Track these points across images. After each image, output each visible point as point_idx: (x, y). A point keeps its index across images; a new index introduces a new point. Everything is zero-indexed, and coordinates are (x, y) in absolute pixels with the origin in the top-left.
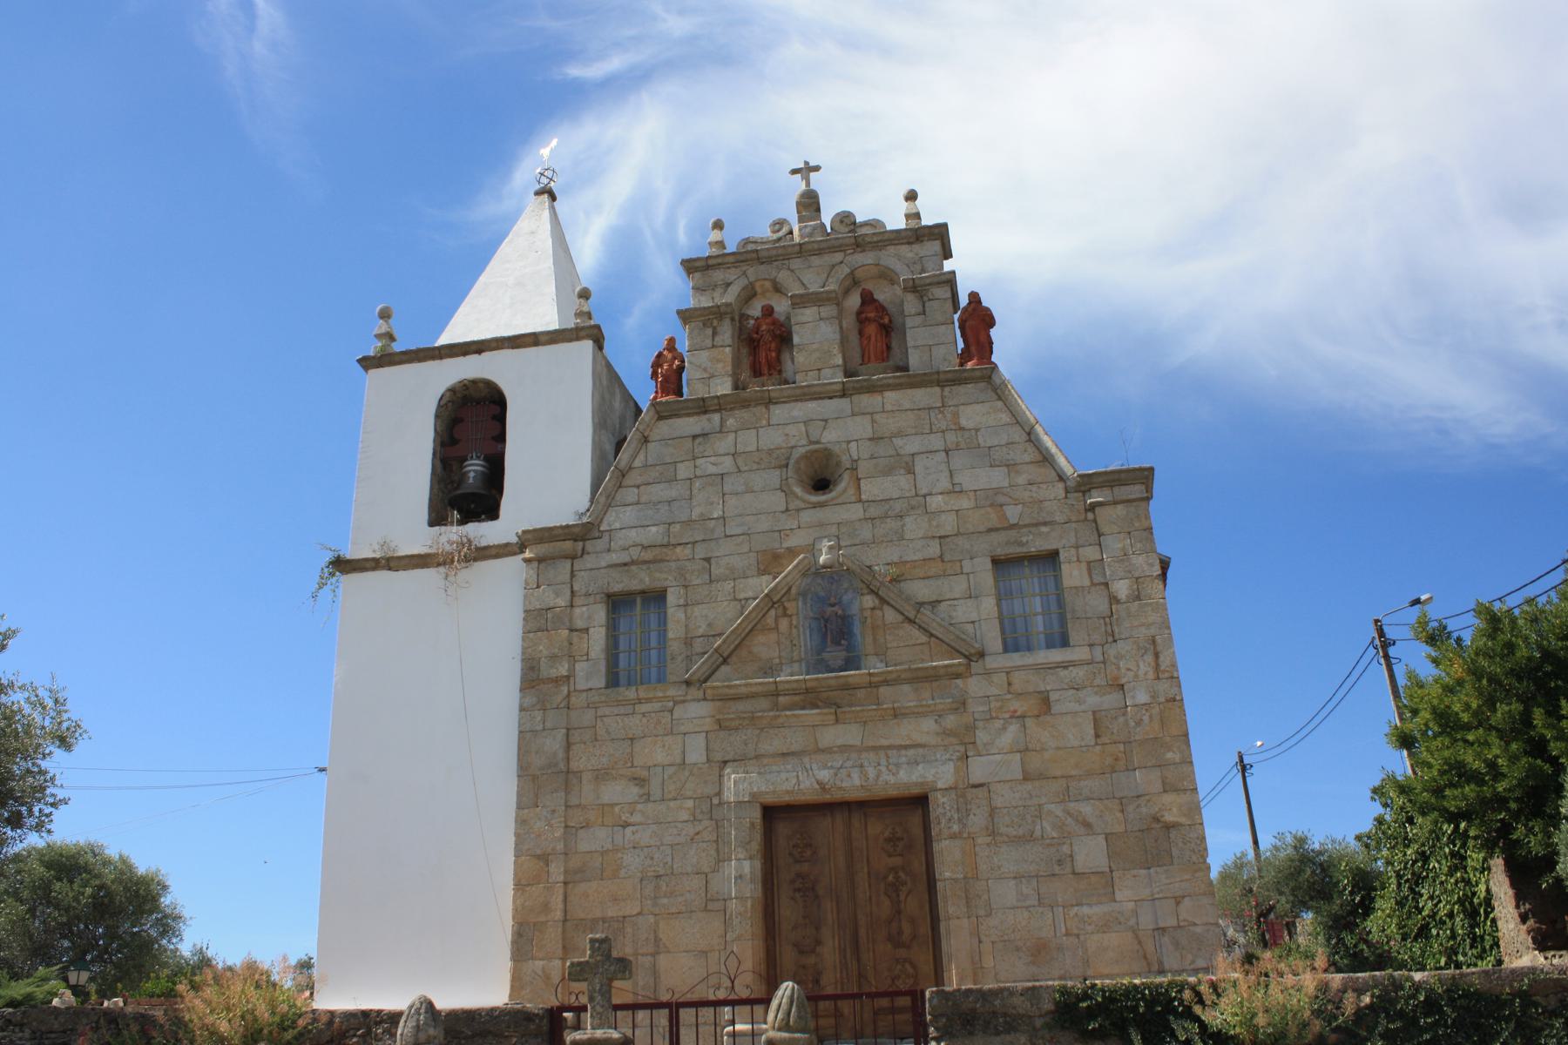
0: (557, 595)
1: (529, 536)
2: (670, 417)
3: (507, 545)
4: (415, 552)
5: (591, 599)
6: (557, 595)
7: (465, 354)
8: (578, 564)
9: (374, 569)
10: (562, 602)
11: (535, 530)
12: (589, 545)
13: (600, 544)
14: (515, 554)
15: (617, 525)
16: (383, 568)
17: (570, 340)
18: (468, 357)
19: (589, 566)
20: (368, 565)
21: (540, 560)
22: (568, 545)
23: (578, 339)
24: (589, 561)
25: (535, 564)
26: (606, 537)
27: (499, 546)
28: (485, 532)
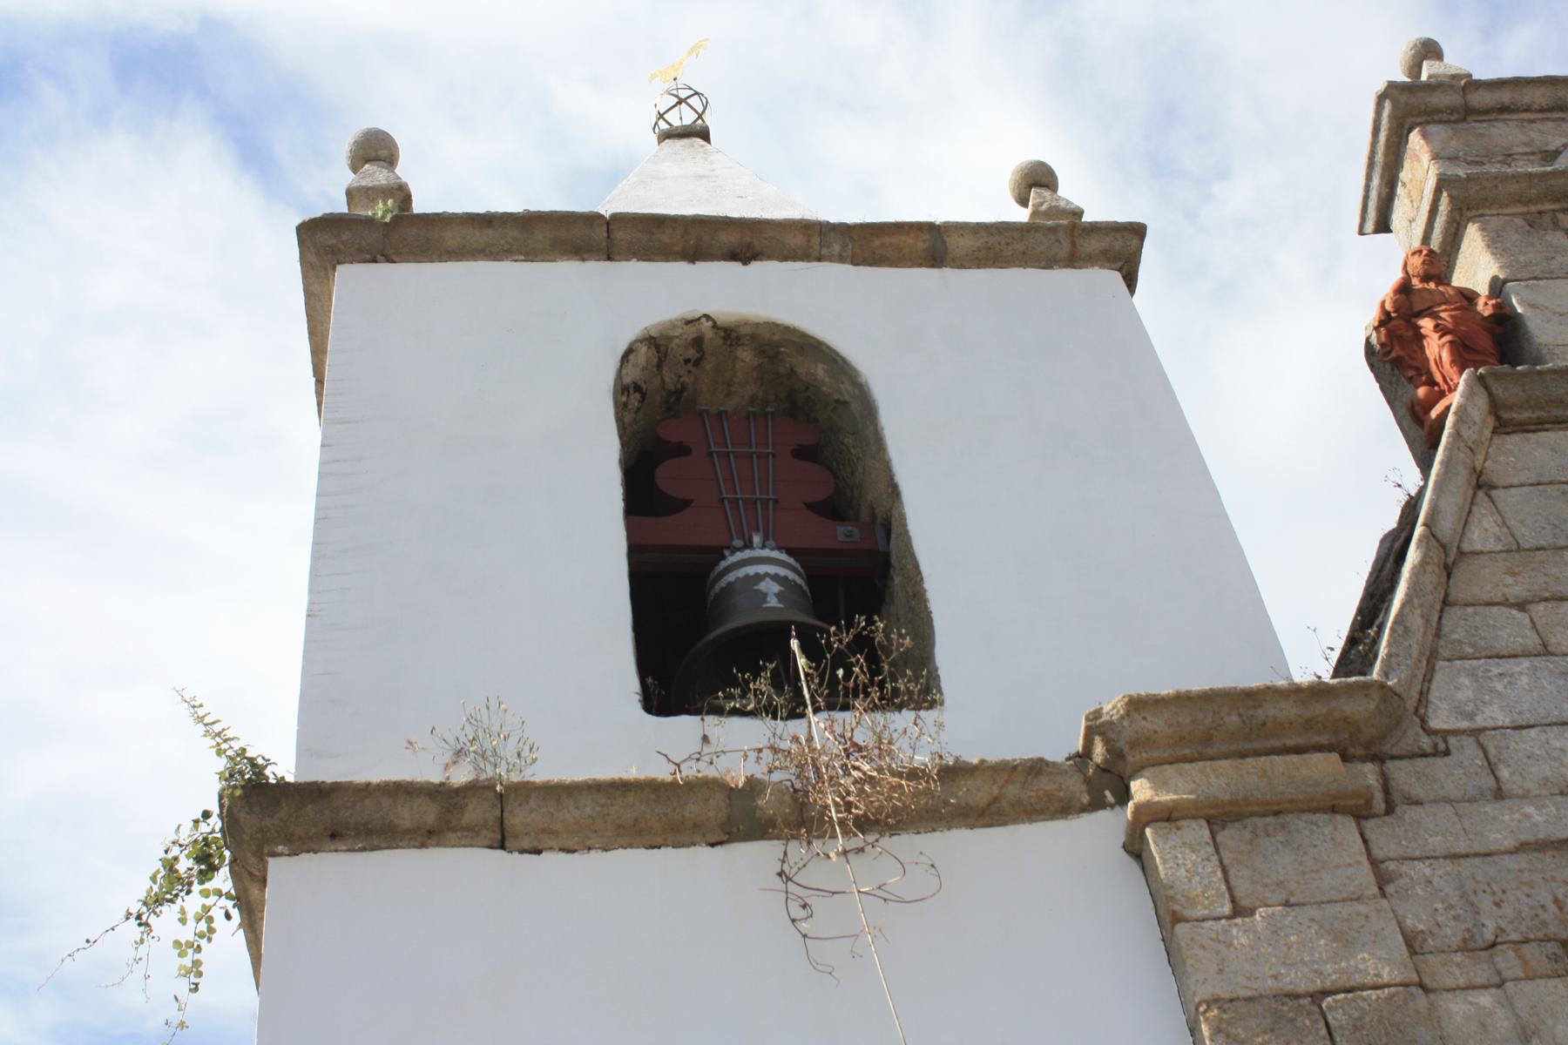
0: (1345, 941)
1: (1155, 723)
2: (1538, 426)
3: (1037, 767)
4: (633, 773)
5: (1506, 960)
6: (1345, 941)
7: (694, 254)
8: (1387, 838)
9: (427, 836)
10: (1379, 963)
11: (1182, 700)
12: (1403, 774)
13: (1457, 772)
14: (1065, 809)
15: (1493, 714)
16: (470, 836)
17: (1049, 263)
18: (700, 265)
19: (1436, 843)
20: (405, 815)
21: (1219, 816)
22: (1323, 768)
23: (1073, 260)
24: (1430, 828)
25: (1202, 831)
26: (1467, 751)
27: (1006, 770)
28: (915, 739)
